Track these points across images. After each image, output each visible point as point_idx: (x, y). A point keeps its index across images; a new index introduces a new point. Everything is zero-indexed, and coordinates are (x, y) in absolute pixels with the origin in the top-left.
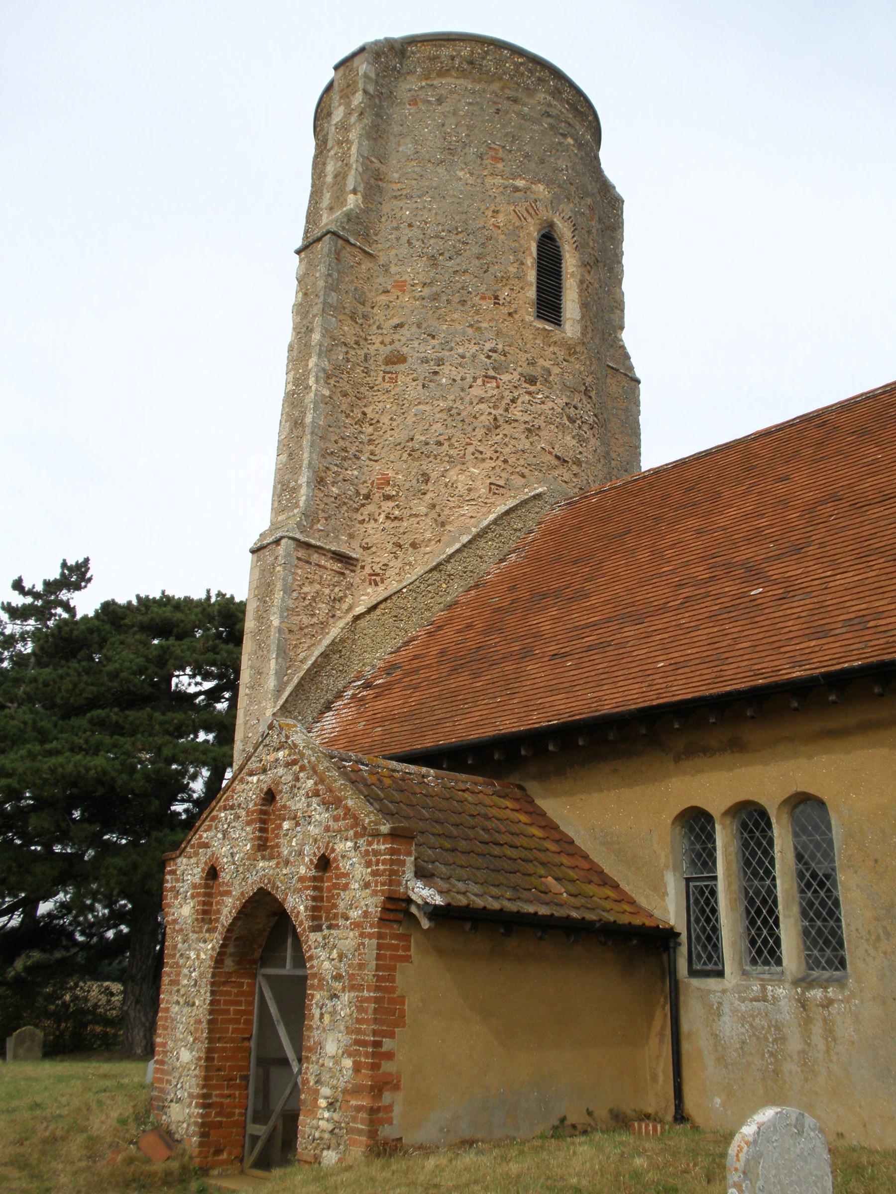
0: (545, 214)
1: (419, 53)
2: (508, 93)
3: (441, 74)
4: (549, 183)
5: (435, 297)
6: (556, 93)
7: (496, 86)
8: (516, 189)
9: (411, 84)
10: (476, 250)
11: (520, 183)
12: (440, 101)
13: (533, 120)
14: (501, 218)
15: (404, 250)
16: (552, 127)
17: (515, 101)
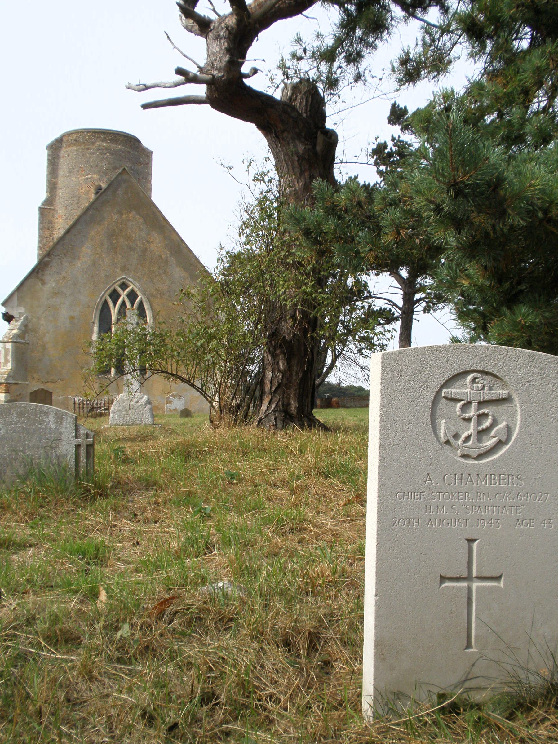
0: (97, 183)
1: (65, 139)
2: (86, 147)
3: (69, 146)
4: (99, 172)
5: (66, 219)
6: (104, 140)
7: (82, 146)
8: (88, 179)
9: (63, 150)
10: (77, 201)
11: (89, 176)
12: (68, 156)
13: (93, 154)
14: (84, 189)
15: (60, 206)
16: (100, 153)
17: (88, 149)
